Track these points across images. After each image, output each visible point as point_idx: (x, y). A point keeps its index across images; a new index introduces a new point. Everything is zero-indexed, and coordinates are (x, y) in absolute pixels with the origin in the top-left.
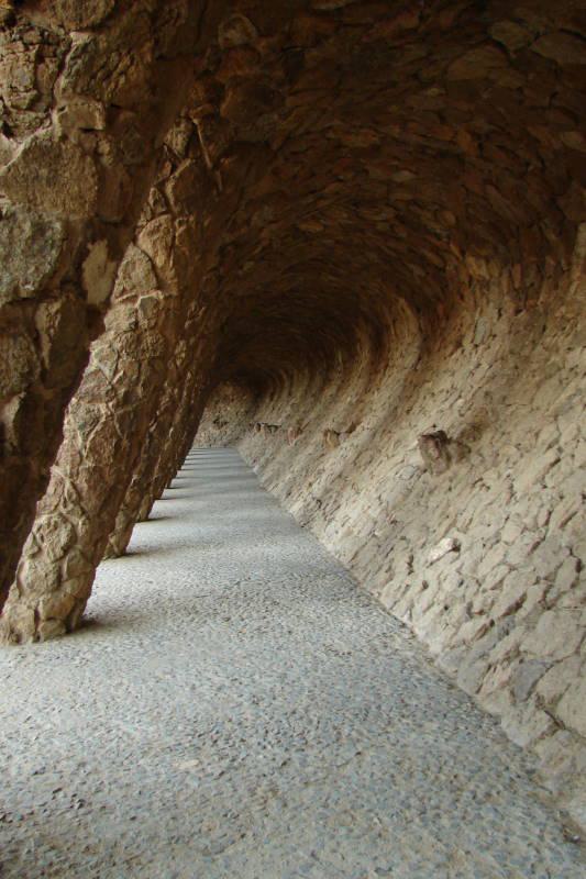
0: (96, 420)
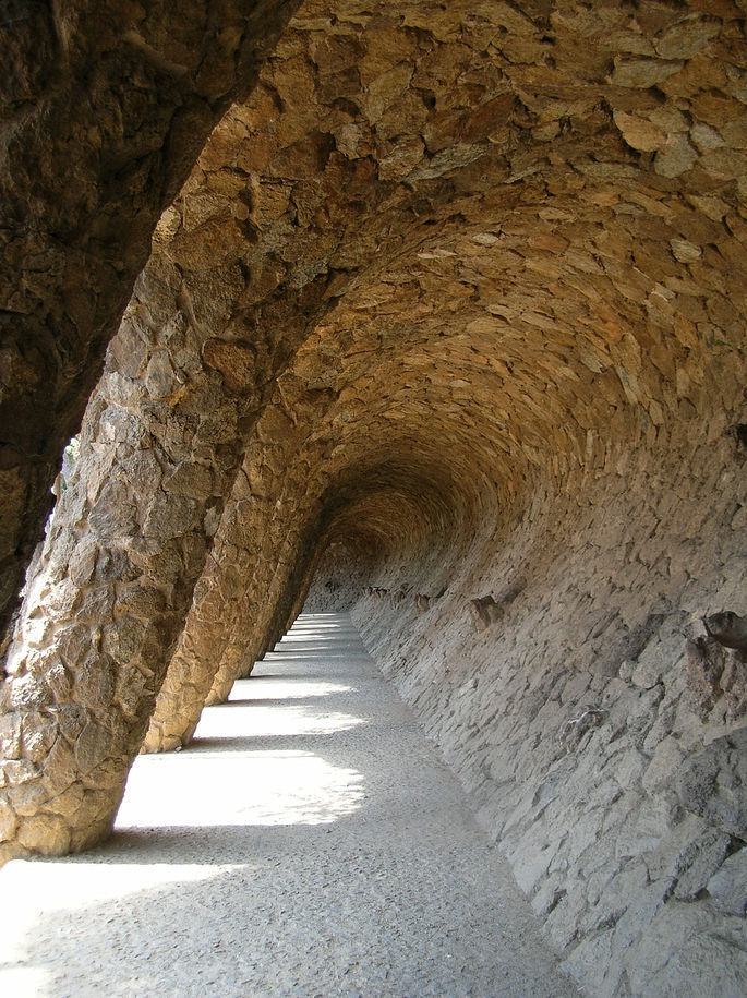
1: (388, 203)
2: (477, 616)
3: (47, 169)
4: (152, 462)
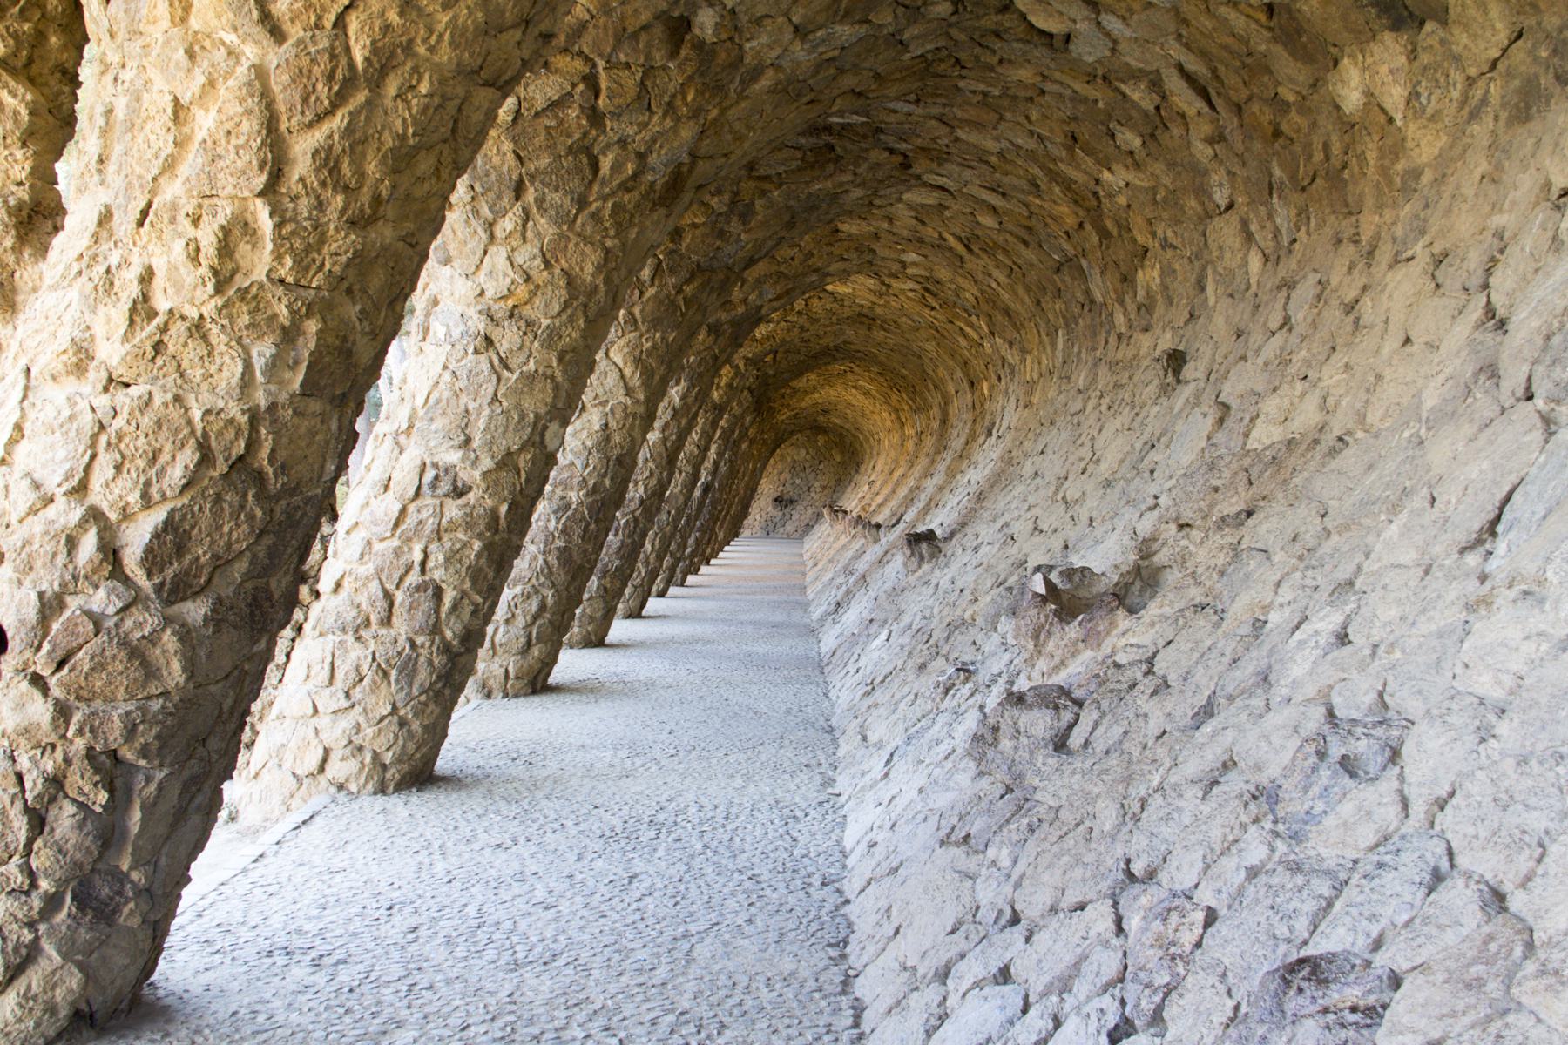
0: (568, 506)
1: (757, 87)
2: (908, 553)
3: (346, 169)
4: (485, 366)
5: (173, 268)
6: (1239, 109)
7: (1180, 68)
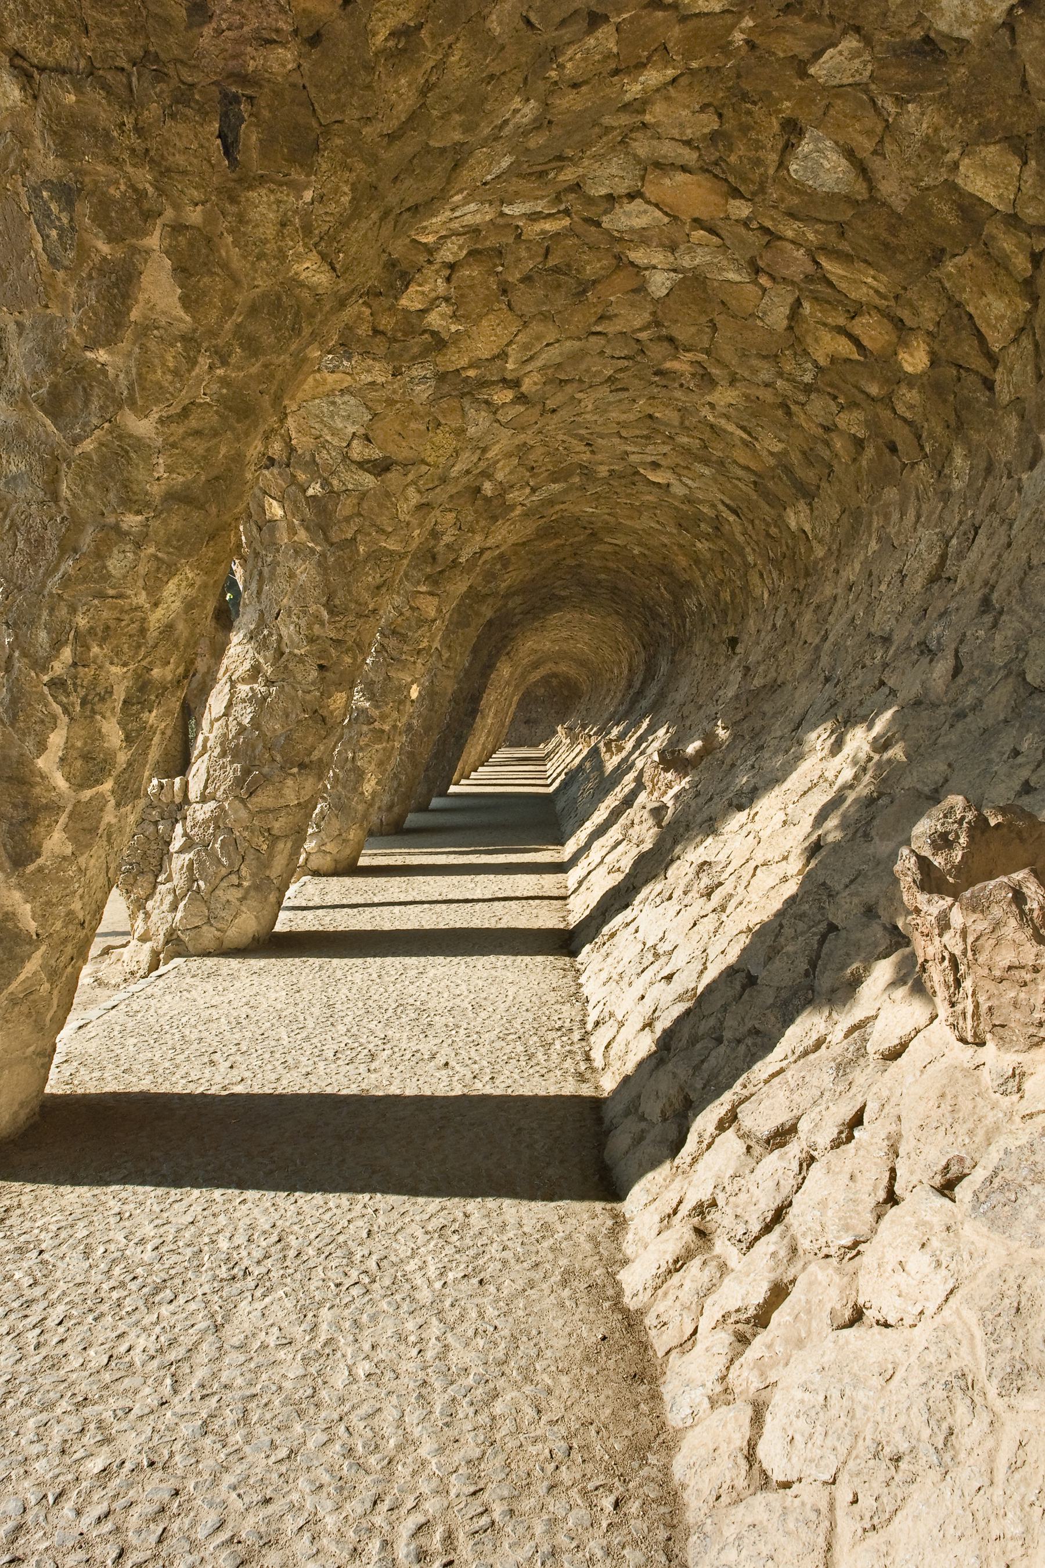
5: (290, 636)
6: (752, 522)
7: (723, 502)
